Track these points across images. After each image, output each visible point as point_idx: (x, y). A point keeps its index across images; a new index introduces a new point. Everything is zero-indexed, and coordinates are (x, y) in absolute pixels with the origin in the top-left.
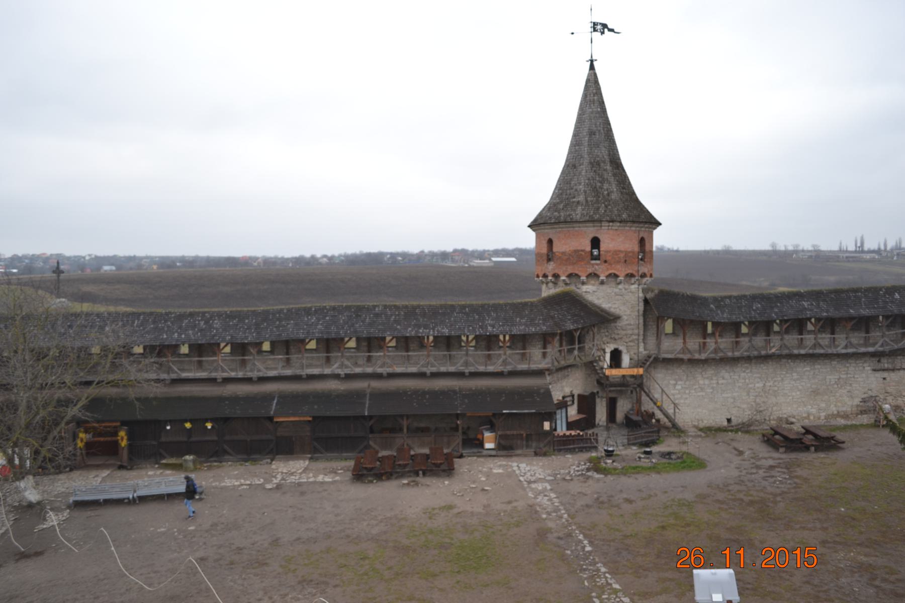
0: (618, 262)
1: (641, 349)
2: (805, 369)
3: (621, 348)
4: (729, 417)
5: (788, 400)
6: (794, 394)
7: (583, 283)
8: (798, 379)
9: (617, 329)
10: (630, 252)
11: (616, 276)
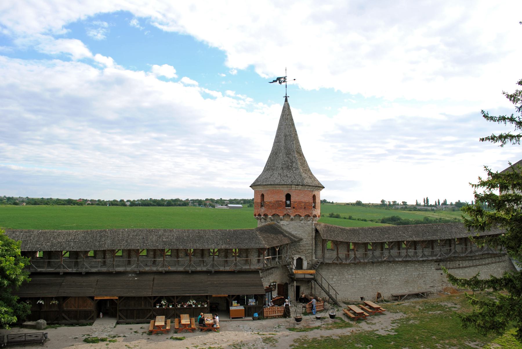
0: (301, 208)
1: (314, 258)
2: (401, 269)
3: (302, 257)
4: (362, 297)
5: (393, 287)
6: (396, 283)
7: (281, 220)
8: (398, 275)
9: (300, 246)
10: (307, 203)
11: (300, 216)
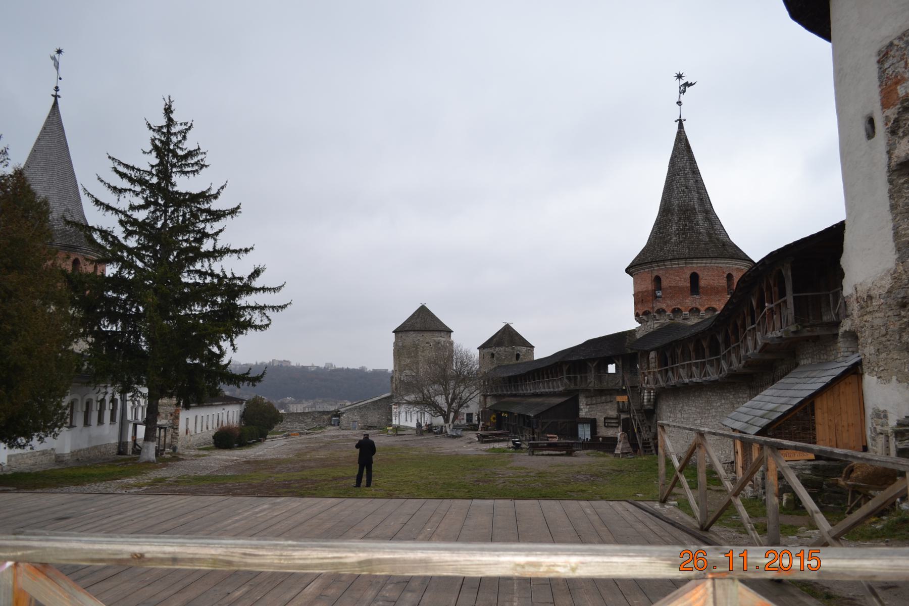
10: (646, 291)
